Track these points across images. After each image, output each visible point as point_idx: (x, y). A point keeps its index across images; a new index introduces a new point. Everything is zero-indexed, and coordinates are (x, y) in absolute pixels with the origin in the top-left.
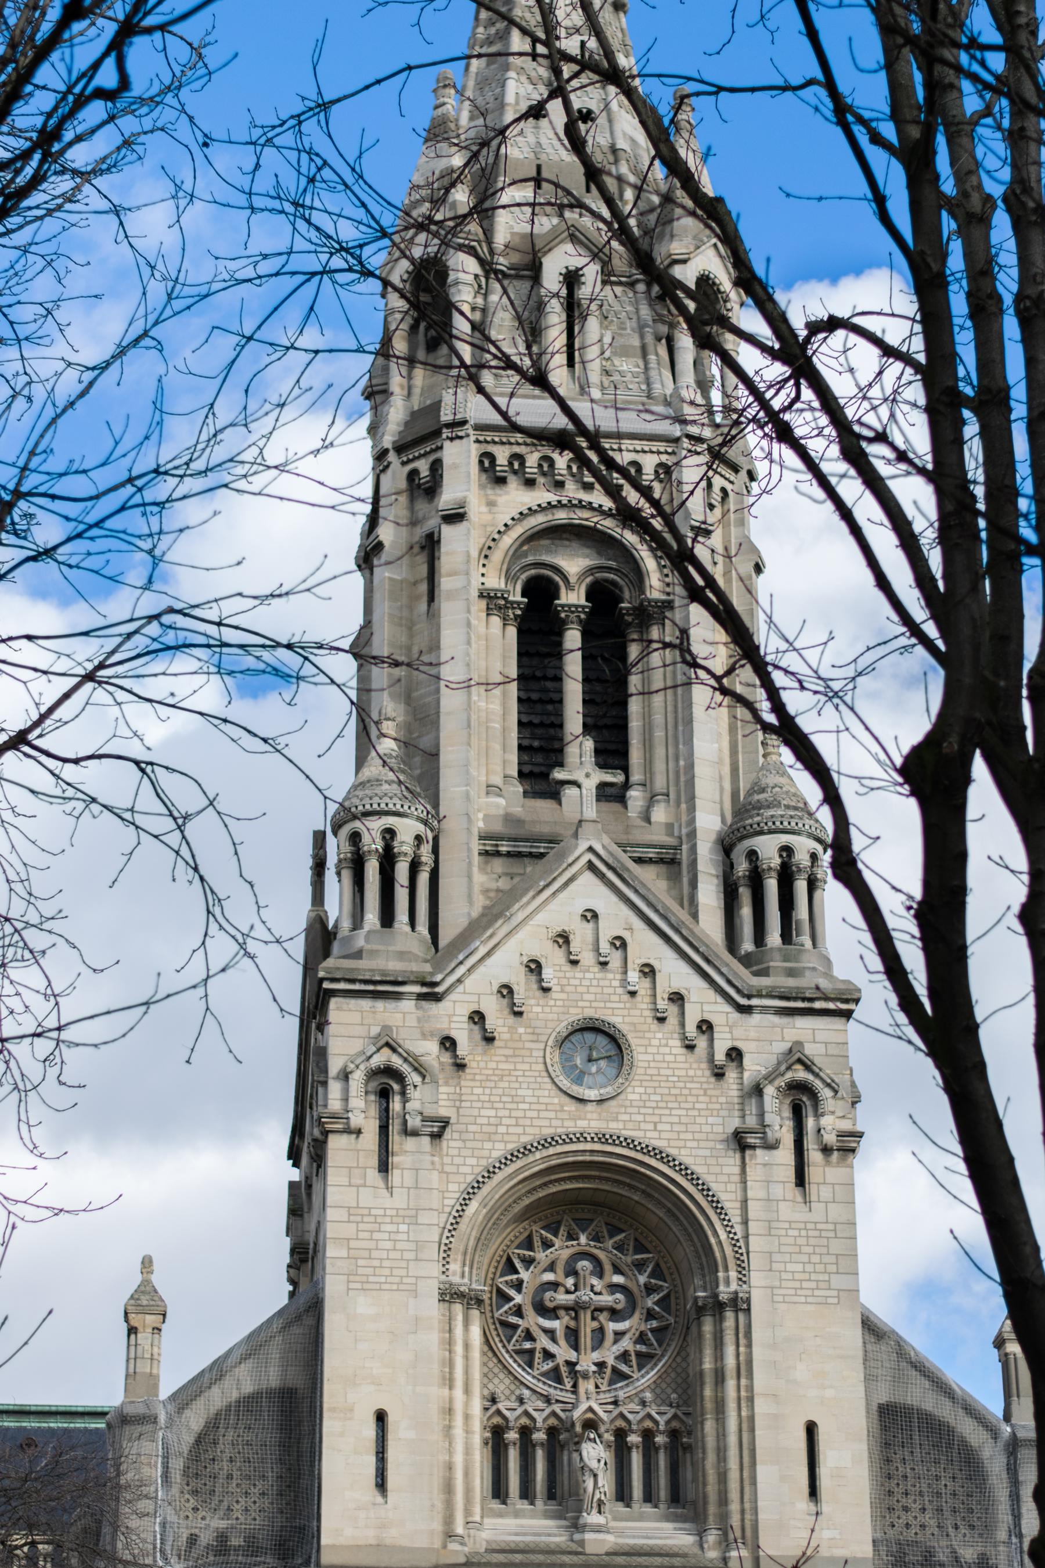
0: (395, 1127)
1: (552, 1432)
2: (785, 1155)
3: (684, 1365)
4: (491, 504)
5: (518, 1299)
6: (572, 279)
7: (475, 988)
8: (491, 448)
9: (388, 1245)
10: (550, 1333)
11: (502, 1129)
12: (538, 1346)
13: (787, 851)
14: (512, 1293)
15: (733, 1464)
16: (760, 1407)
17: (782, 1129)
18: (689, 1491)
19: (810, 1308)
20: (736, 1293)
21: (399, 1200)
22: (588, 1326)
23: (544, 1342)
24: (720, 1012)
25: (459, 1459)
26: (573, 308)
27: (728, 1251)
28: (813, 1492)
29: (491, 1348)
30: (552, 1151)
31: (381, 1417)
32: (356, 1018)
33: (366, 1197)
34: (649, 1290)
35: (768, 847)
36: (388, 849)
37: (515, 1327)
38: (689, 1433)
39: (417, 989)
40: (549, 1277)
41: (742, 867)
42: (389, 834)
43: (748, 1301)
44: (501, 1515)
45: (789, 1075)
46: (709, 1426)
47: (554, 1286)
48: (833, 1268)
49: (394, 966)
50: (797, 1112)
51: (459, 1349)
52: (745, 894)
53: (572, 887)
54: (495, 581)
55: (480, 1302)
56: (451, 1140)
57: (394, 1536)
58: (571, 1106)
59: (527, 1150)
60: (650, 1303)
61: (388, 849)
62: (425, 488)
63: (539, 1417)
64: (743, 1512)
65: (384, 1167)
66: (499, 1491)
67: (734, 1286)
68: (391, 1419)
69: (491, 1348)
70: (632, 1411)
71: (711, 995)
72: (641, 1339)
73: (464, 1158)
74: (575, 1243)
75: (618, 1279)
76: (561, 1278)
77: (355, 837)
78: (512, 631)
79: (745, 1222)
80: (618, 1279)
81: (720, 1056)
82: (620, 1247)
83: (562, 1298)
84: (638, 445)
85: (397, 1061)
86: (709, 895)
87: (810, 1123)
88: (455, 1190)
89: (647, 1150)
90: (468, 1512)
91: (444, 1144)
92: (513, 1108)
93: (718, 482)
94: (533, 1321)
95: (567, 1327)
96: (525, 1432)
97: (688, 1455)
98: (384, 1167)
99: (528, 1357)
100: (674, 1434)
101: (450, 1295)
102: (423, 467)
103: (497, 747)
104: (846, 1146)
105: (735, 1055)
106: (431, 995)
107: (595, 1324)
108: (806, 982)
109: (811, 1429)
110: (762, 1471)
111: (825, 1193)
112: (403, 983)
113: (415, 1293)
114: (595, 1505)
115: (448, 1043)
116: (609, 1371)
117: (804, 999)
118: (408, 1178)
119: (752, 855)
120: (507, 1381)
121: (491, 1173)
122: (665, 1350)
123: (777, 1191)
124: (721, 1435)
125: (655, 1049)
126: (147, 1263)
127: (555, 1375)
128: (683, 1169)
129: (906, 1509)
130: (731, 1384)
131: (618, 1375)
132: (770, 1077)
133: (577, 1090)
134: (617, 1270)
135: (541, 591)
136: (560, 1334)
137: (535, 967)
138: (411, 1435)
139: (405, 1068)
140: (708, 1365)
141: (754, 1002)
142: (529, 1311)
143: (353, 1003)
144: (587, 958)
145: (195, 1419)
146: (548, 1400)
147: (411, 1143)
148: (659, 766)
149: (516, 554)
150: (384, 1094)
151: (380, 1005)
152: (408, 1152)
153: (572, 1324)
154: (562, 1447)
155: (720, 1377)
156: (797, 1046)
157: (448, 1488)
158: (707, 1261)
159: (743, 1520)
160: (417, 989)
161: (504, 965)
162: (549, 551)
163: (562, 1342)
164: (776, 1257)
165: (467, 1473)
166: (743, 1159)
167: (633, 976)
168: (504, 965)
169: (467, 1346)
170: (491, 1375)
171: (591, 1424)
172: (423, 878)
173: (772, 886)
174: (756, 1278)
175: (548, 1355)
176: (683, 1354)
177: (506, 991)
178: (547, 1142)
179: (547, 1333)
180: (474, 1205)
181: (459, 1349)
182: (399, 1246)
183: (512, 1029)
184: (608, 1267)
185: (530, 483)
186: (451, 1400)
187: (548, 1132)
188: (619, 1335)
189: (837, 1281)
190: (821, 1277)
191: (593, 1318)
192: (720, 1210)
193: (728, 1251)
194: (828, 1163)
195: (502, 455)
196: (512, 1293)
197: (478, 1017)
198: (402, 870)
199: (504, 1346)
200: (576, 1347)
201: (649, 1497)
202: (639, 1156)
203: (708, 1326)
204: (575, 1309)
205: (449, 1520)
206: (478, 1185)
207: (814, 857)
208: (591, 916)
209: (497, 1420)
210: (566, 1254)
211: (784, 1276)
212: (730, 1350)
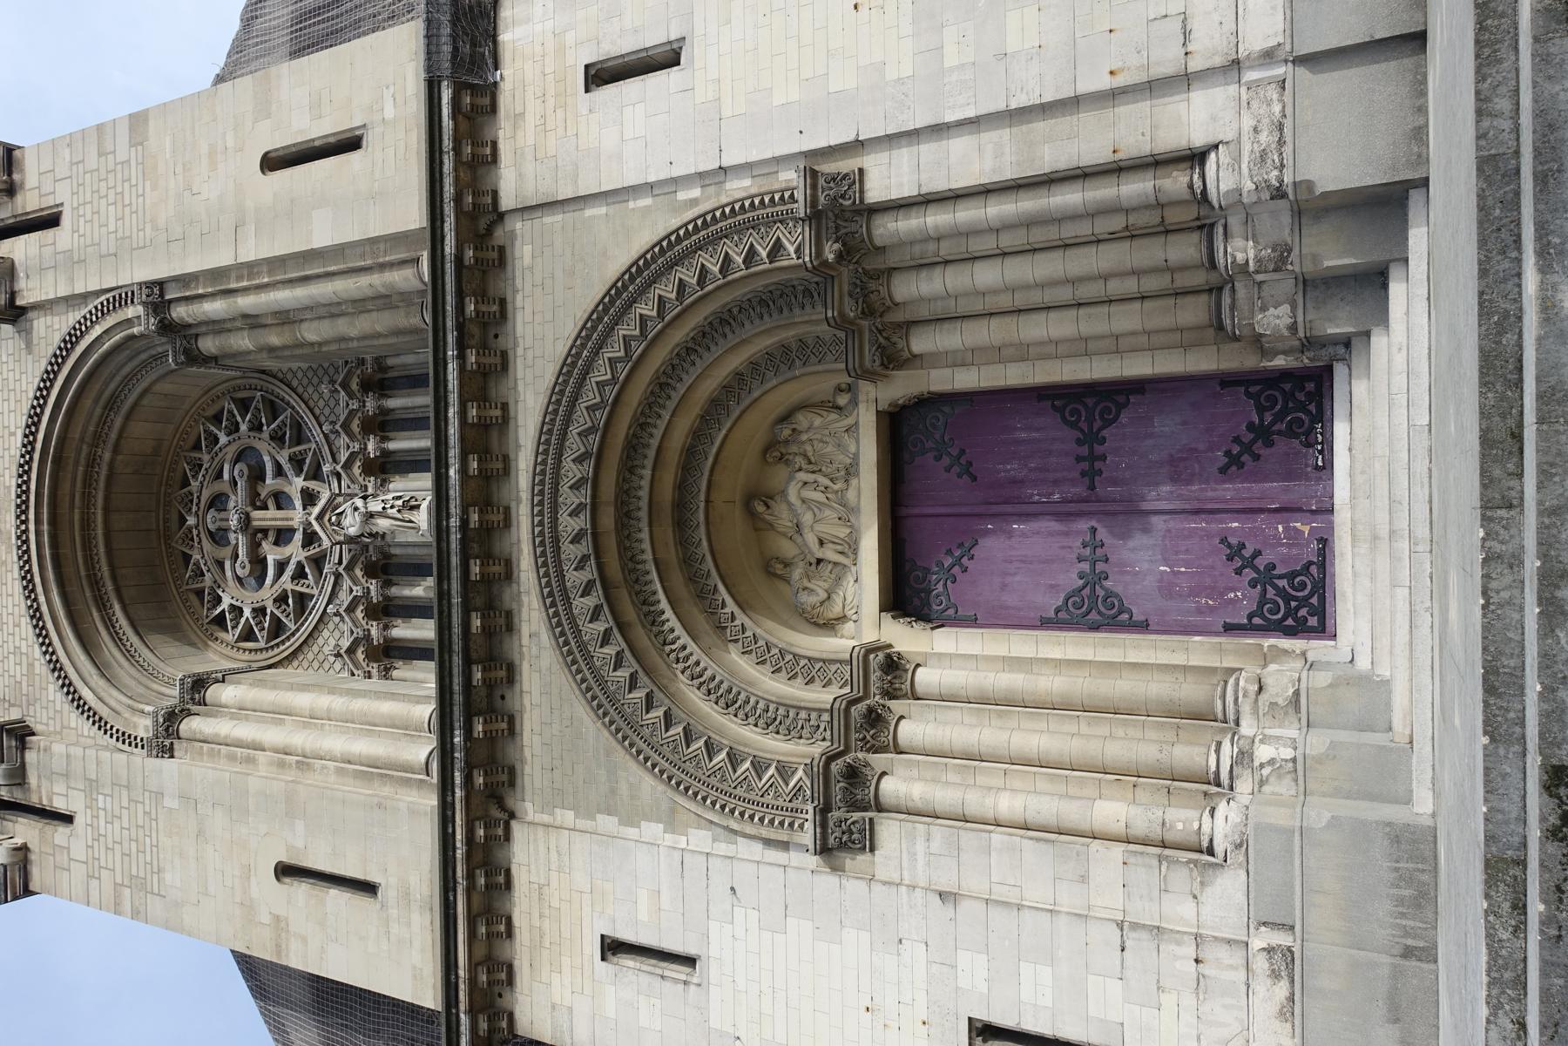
1: (370, 572)
3: (300, 375)
5: (247, 612)
10: (281, 566)
11: (24, 650)
12: (289, 586)
16: (251, 251)
19: (148, 189)
20: (144, 304)
22: (268, 517)
27: (110, 321)
29: (294, 654)
30: (37, 580)
31: (286, 871)
33: (78, 852)
34: (235, 428)
43: (150, 285)
46: (312, 332)
48: (110, 157)
55: (199, 684)
59: (36, 615)
60: (243, 427)
63: (358, 591)
64: (382, 267)
67: (140, 310)
69: (294, 654)
72: (278, 438)
74: (195, 532)
75: (226, 476)
76: (228, 551)
79: (85, 297)
88: (74, 719)
89: (29, 446)
91: (38, 728)
95: (276, 543)
96: (374, 612)
97: (390, 362)
107: (271, 503)
109: (271, 163)
110: (321, 240)
113: (159, 795)
114: (407, 515)
116: (312, 485)
118: (59, 788)
120: (326, 633)
122: (288, 404)
130: (246, 303)
134: (219, 475)
138: (300, 826)
146: (338, 576)
147: (32, 779)
153: (271, 538)
154: (387, 556)
155: (252, 321)
159: (391, 265)
163: (287, 551)
164: (104, 251)
166: (36, 307)
170: (321, 657)
174: (124, 279)
175: (300, 574)
176: (289, 376)
180: (86, 693)
182: (117, 812)
184: (219, 487)
186: (277, 751)
189: (123, 152)
190: (119, 176)
191: (265, 508)
193: (110, 321)
199: (293, 634)
200: (292, 531)
202: (36, 456)
203: (208, 345)
204: (257, 536)
206: (67, 686)
211: (120, 234)
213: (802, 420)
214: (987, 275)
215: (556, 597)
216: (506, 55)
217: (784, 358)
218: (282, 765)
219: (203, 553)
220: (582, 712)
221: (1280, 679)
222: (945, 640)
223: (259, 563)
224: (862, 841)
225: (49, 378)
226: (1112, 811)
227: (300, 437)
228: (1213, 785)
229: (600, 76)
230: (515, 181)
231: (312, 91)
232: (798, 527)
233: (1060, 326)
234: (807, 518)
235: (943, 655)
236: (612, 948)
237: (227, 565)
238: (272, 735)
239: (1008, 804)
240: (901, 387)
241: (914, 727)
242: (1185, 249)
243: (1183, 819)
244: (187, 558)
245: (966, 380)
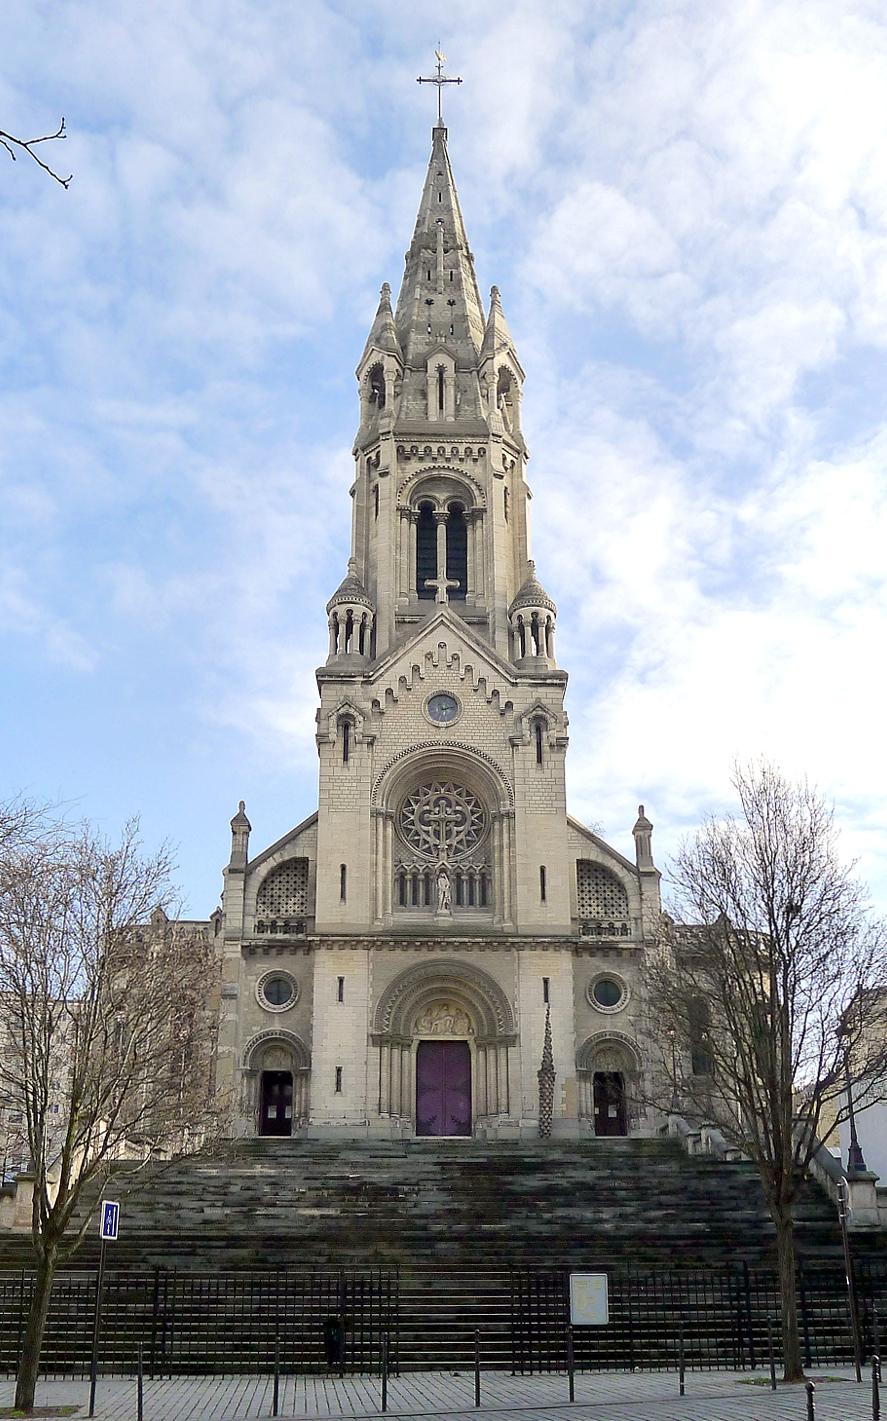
0: (351, 740)
1: (427, 875)
2: (533, 749)
4: (403, 469)
6: (441, 370)
7: (389, 679)
8: (402, 444)
9: (348, 792)
10: (427, 832)
13: (535, 614)
14: (409, 815)
15: (506, 886)
16: (519, 860)
17: (529, 735)
18: (489, 899)
21: (353, 772)
22: (443, 830)
23: (424, 836)
24: (503, 686)
25: (380, 885)
26: (441, 381)
28: (543, 897)
30: (424, 750)
31: (343, 868)
32: (334, 693)
34: (473, 813)
35: (526, 613)
36: (350, 618)
37: (411, 830)
38: (490, 875)
39: (362, 679)
40: (427, 808)
41: (516, 622)
42: (350, 612)
44: (403, 911)
45: (534, 712)
47: (429, 812)
49: (351, 669)
50: (538, 730)
51: (381, 838)
53: (434, 632)
54: (405, 503)
55: (392, 817)
56: (377, 747)
57: (349, 919)
58: (434, 730)
59: (412, 750)
61: (350, 618)
62: (373, 465)
63: (421, 869)
65: (346, 759)
66: (402, 901)
68: (347, 868)
70: (465, 866)
71: (499, 678)
72: (469, 834)
73: (384, 753)
75: (458, 808)
77: (335, 614)
78: (414, 527)
80: (458, 808)
81: (503, 706)
82: (460, 794)
83: (432, 817)
84: (470, 440)
85: (352, 711)
86: (501, 637)
87: (544, 735)
88: (379, 769)
90: (385, 909)
92: (407, 731)
93: (509, 458)
94: (419, 827)
96: (415, 876)
98: (346, 759)
99: (417, 843)
100: (483, 876)
101: (376, 814)
102: (373, 456)
103: (405, 576)
104: (561, 744)
105: (509, 705)
106: (368, 682)
108: (542, 672)
109: (543, 870)
111: (551, 765)
112: (354, 677)
115: (376, 703)
117: (541, 679)
121: (396, 760)
123: (528, 765)
124: (502, 874)
125: (473, 705)
126: (242, 804)
127: (428, 850)
128: (485, 757)
129: (590, 906)
130: (506, 850)
131: (457, 851)
132: (524, 715)
133: (436, 723)
135: (427, 509)
136: (431, 832)
137: (416, 669)
139: (356, 714)
140: (496, 844)
141: (518, 681)
142: (417, 823)
143: (332, 686)
144: (443, 665)
145: (263, 870)
148: (479, 582)
149: (415, 491)
150: (346, 727)
151: (344, 687)
152: (358, 752)
157: (375, 899)
158: (497, 798)
160: (362, 679)
161: (403, 668)
162: (430, 490)
165: (385, 892)
167: (462, 671)
168: (403, 668)
169: (385, 837)
171: (443, 871)
173: (528, 630)
174: (517, 804)
175: (426, 842)
177: (403, 680)
178: (423, 746)
179: (426, 833)
180: (388, 774)
181: (381, 838)
183: (406, 697)
184: (454, 803)
185: (421, 459)
187: (422, 741)
188: (458, 833)
192: (501, 774)
194: (553, 752)
196: (409, 815)
197: (389, 692)
198: (356, 628)
201: (471, 903)
202: (464, 751)
205: (376, 911)
207: (549, 617)
208: (442, 646)
209: (402, 870)
210: (435, 797)
212: (505, 836)
213: (467, 1020)
214: (492, 1070)
215: (425, 965)
216: (557, 954)
217: (480, 1022)
218: (372, 865)
219: (432, 796)
220: (396, 972)
221: (409, 1125)
222: (414, 1056)
223: (428, 824)
224: (374, 1044)
225: (490, 761)
226: (385, 1095)
227: (469, 844)
228: (390, 1113)
229: (546, 981)
230: (526, 953)
231: (562, 881)
232: (440, 1019)
233: (482, 1085)
234: (442, 1021)
235: (411, 1057)
236: (341, 980)
237: (427, 808)
238: (380, 856)
239: (384, 1075)
240: (473, 1047)
241: (396, 1052)
242: (494, 1110)
243: (385, 1108)
244: (429, 786)
245: (473, 1061)
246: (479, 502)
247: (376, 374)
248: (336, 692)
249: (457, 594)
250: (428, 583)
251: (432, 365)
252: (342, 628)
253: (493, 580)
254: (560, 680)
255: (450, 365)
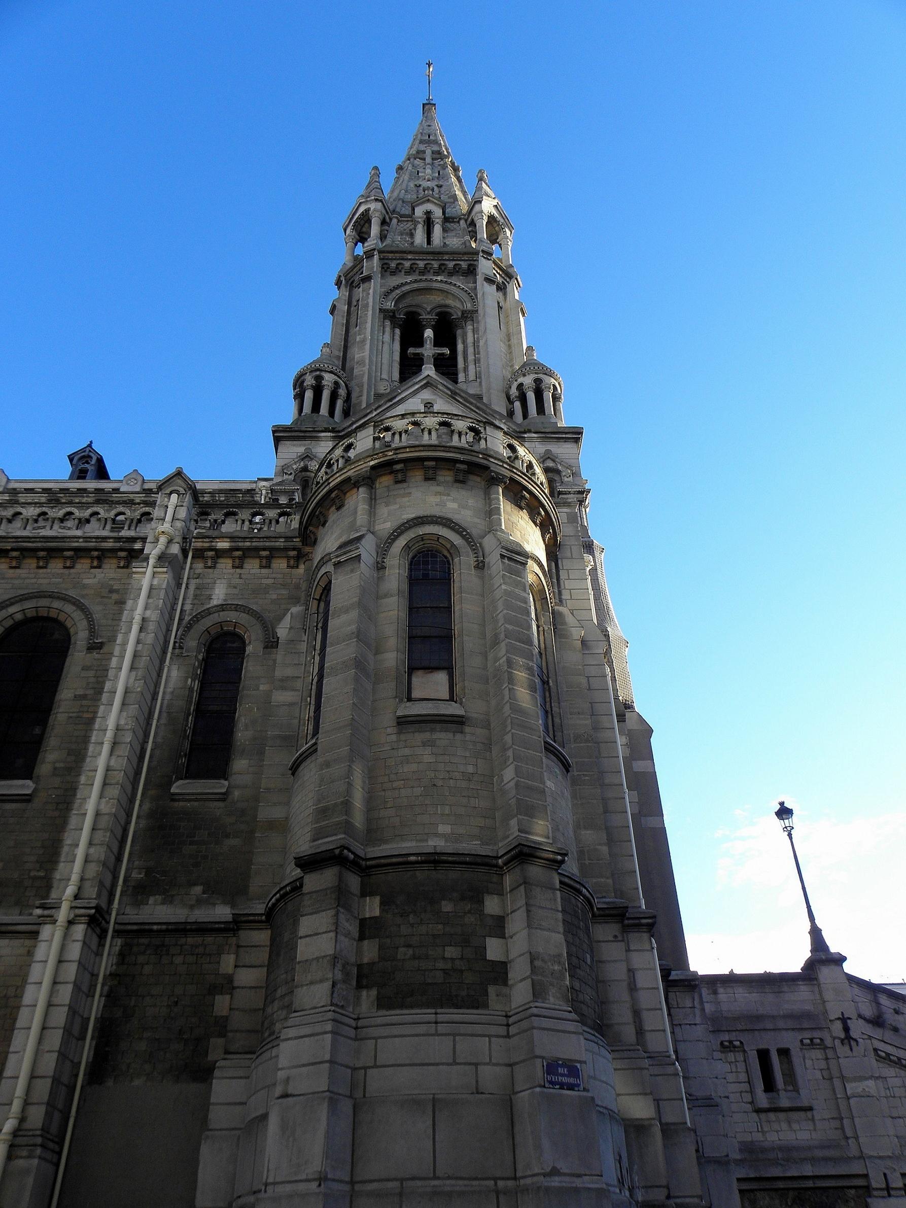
41: (514, 392)
52: (517, 404)
78: (398, 331)
119: (521, 385)
156: (548, 452)
172: (339, 404)
173: (531, 397)
185: (408, 273)
195: (393, 265)
198: (326, 395)
246: (469, 306)
247: (365, 219)
248: (293, 450)
249: (447, 367)
250: (411, 350)
251: (419, 211)
252: (309, 395)
253: (489, 357)
254: (574, 435)
255: (438, 212)
